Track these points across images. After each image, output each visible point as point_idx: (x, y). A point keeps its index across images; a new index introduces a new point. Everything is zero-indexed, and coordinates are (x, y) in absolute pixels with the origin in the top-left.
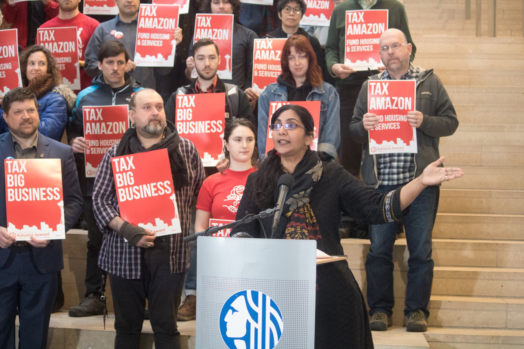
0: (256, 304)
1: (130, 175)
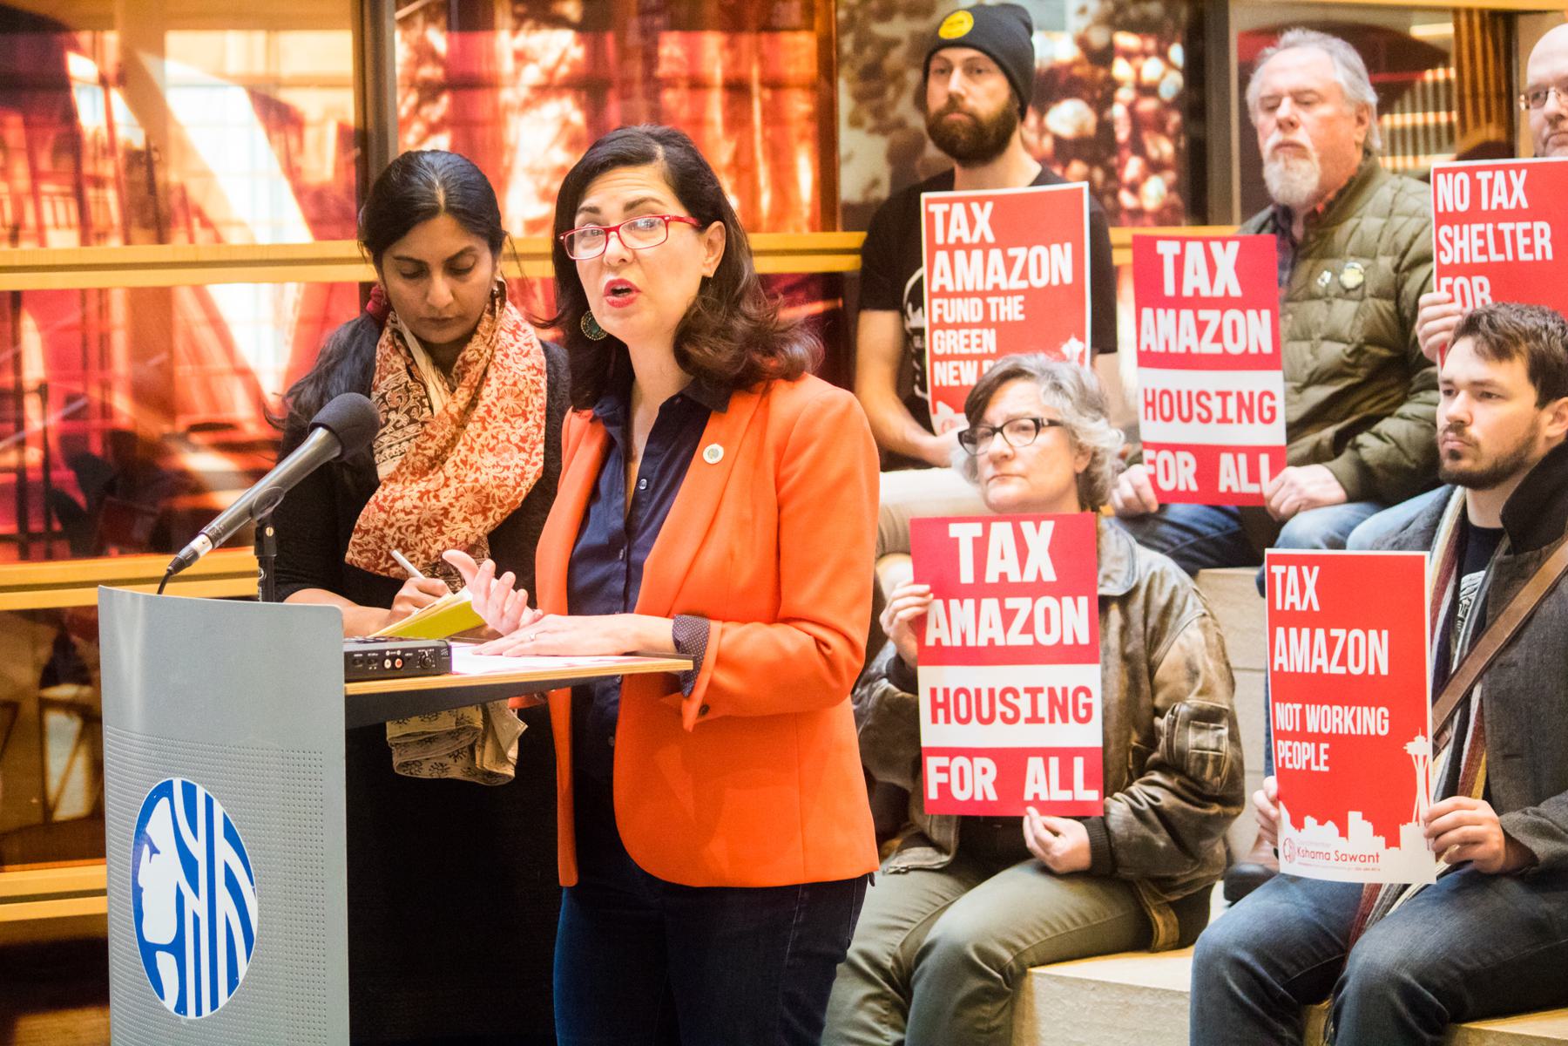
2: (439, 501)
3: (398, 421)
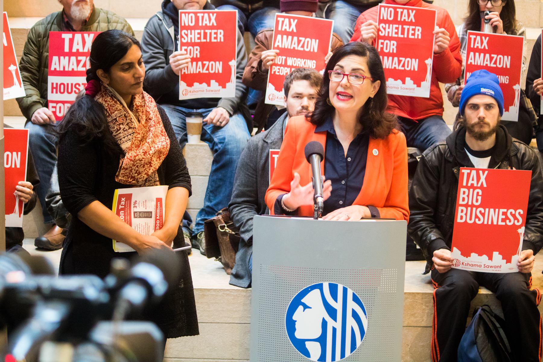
0: (335, 298)
1: (478, 193)
2: (150, 155)
3: (124, 128)
